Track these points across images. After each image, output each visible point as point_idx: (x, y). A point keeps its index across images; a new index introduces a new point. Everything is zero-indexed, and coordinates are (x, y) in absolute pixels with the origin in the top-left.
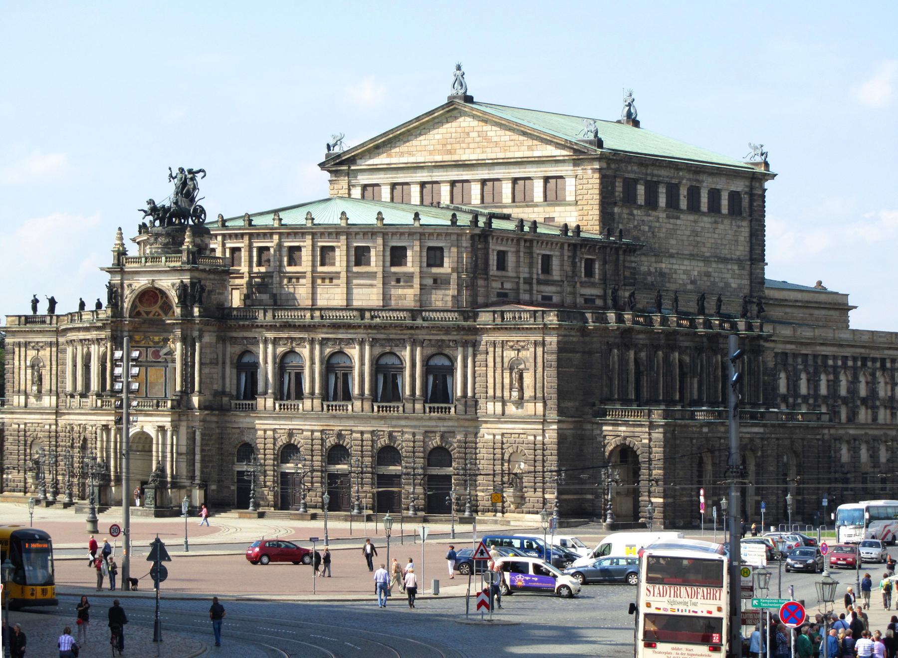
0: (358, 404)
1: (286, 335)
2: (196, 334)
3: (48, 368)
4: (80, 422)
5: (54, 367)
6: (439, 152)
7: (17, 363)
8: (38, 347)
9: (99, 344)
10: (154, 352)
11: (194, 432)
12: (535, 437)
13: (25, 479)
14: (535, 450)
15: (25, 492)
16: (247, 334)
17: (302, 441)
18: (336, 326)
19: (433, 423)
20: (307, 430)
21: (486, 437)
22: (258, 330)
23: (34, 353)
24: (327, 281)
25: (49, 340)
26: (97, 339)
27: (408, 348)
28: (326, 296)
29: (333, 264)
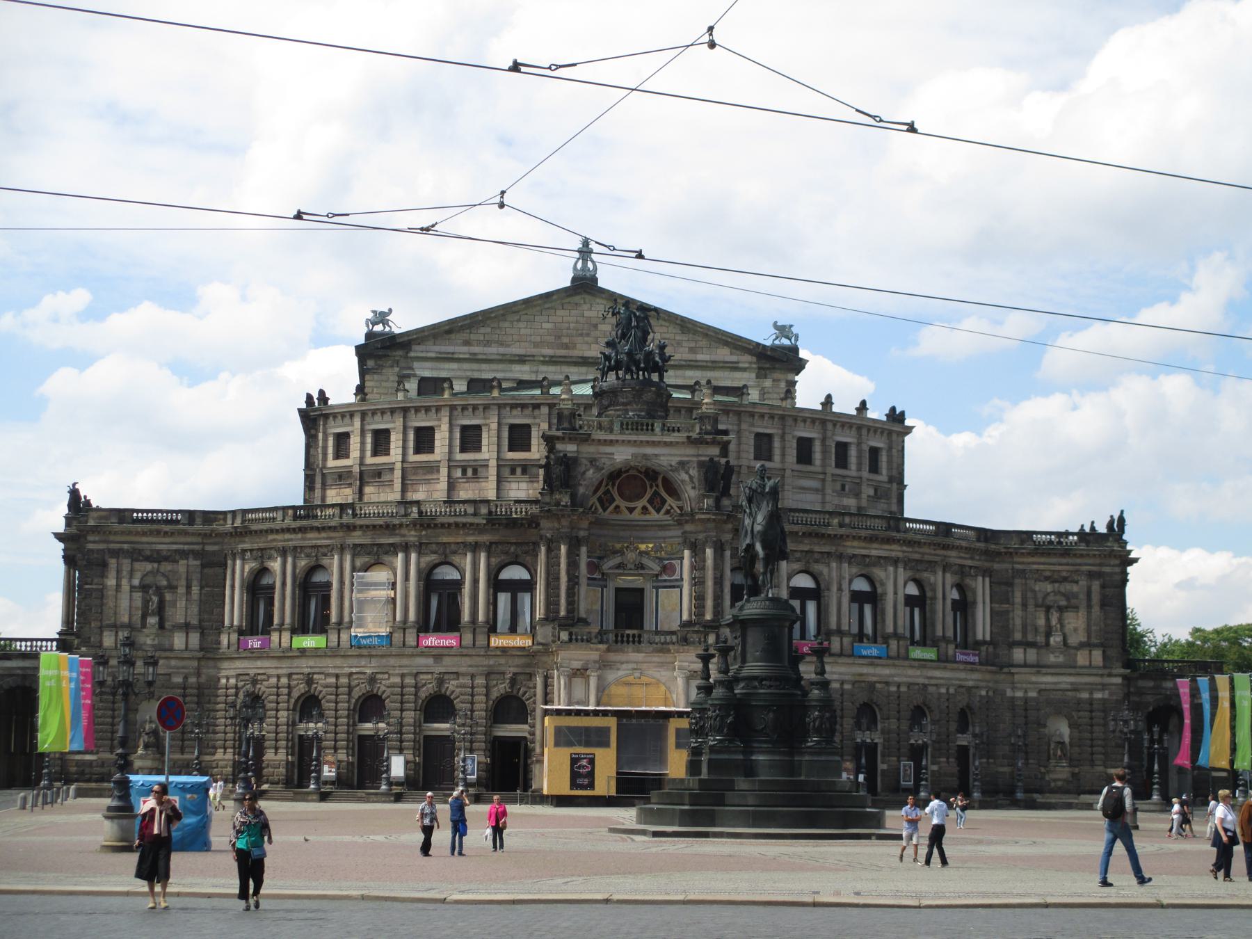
0: (893, 644)
3: (181, 590)
4: (354, 670)
5: (195, 590)
6: (550, 345)
7: (111, 582)
8: (157, 557)
12: (1091, 693)
14: (1091, 711)
18: (872, 539)
19: (962, 675)
20: (836, 681)
21: (1009, 693)
23: (149, 566)
25: (186, 547)
26: (421, 544)
27: (940, 573)
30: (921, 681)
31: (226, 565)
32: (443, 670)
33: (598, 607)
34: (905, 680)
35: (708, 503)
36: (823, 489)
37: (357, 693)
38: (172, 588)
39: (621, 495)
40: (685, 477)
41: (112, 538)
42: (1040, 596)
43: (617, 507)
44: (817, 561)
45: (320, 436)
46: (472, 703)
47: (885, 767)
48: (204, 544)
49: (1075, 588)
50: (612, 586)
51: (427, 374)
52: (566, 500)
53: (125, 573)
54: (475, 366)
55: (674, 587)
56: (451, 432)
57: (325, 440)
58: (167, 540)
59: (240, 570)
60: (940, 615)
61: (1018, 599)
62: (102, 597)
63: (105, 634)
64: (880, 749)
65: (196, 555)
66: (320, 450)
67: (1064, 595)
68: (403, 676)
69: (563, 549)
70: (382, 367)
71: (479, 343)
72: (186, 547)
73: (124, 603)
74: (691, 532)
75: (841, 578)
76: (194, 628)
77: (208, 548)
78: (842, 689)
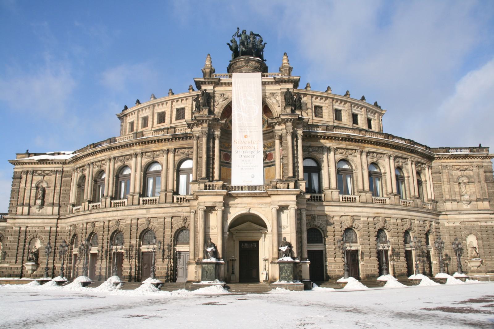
0: (392, 197)
1: (344, 147)
2: (300, 132)
3: (53, 188)
4: (111, 219)
5: (58, 188)
7: (23, 185)
9: (142, 157)
10: (225, 154)
13: (23, 266)
15: (21, 277)
17: (361, 226)
23: (40, 178)
25: (56, 169)
26: (142, 153)
29: (322, 117)
32: (150, 216)
34: (400, 216)
35: (288, 110)
38: (48, 187)
41: (25, 166)
42: (455, 177)
45: (124, 124)
49: (471, 173)
52: (205, 112)
55: (272, 165)
56: (172, 112)
57: (126, 126)
59: (76, 176)
61: (445, 180)
62: (19, 191)
63: (18, 208)
67: (466, 176)
68: (131, 220)
69: (204, 140)
73: (27, 194)
74: (279, 130)
77: (64, 169)
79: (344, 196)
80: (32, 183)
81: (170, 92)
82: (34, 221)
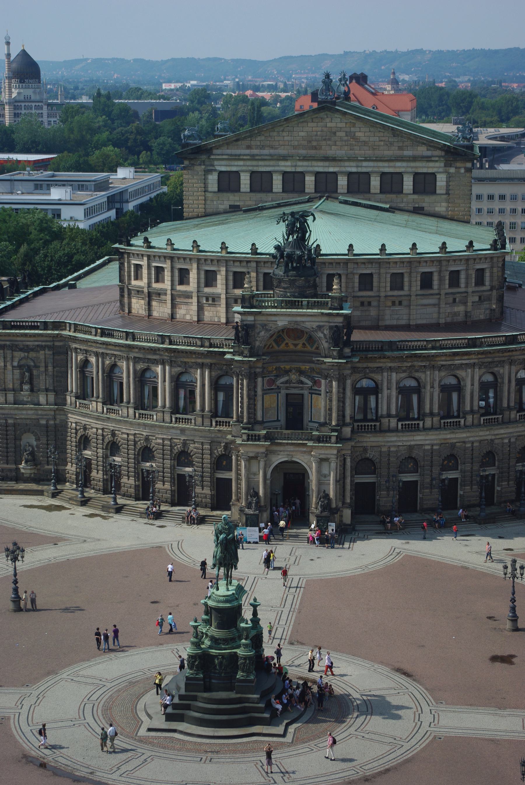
1: (409, 364)
3: (42, 369)
4: (137, 432)
5: (50, 368)
11: (345, 460)
16: (370, 365)
20: (428, 445)
22: (382, 360)
23: (22, 354)
24: (397, 303)
25: (43, 343)
26: (171, 361)
27: (507, 367)
28: (396, 317)
29: (402, 288)
30: (489, 438)
31: (67, 353)
33: (275, 405)
34: (477, 438)
36: (439, 304)
37: (139, 446)
39: (289, 337)
40: (321, 335)
43: (287, 344)
44: (417, 371)
45: (126, 264)
46: (202, 459)
47: (462, 493)
48: (53, 341)
50: (283, 392)
51: (223, 169)
53: (8, 359)
54: (254, 163)
56: (198, 274)
57: (129, 267)
58: (32, 339)
60: (506, 394)
64: (459, 481)
65: (49, 348)
66: (126, 273)
70: (193, 165)
71: (257, 147)
72: (43, 343)
75: (434, 380)
76: (51, 391)
77: (57, 344)
78: (432, 449)
79: (404, 423)
80: (12, 361)
81: (195, 245)
82: (24, 412)
